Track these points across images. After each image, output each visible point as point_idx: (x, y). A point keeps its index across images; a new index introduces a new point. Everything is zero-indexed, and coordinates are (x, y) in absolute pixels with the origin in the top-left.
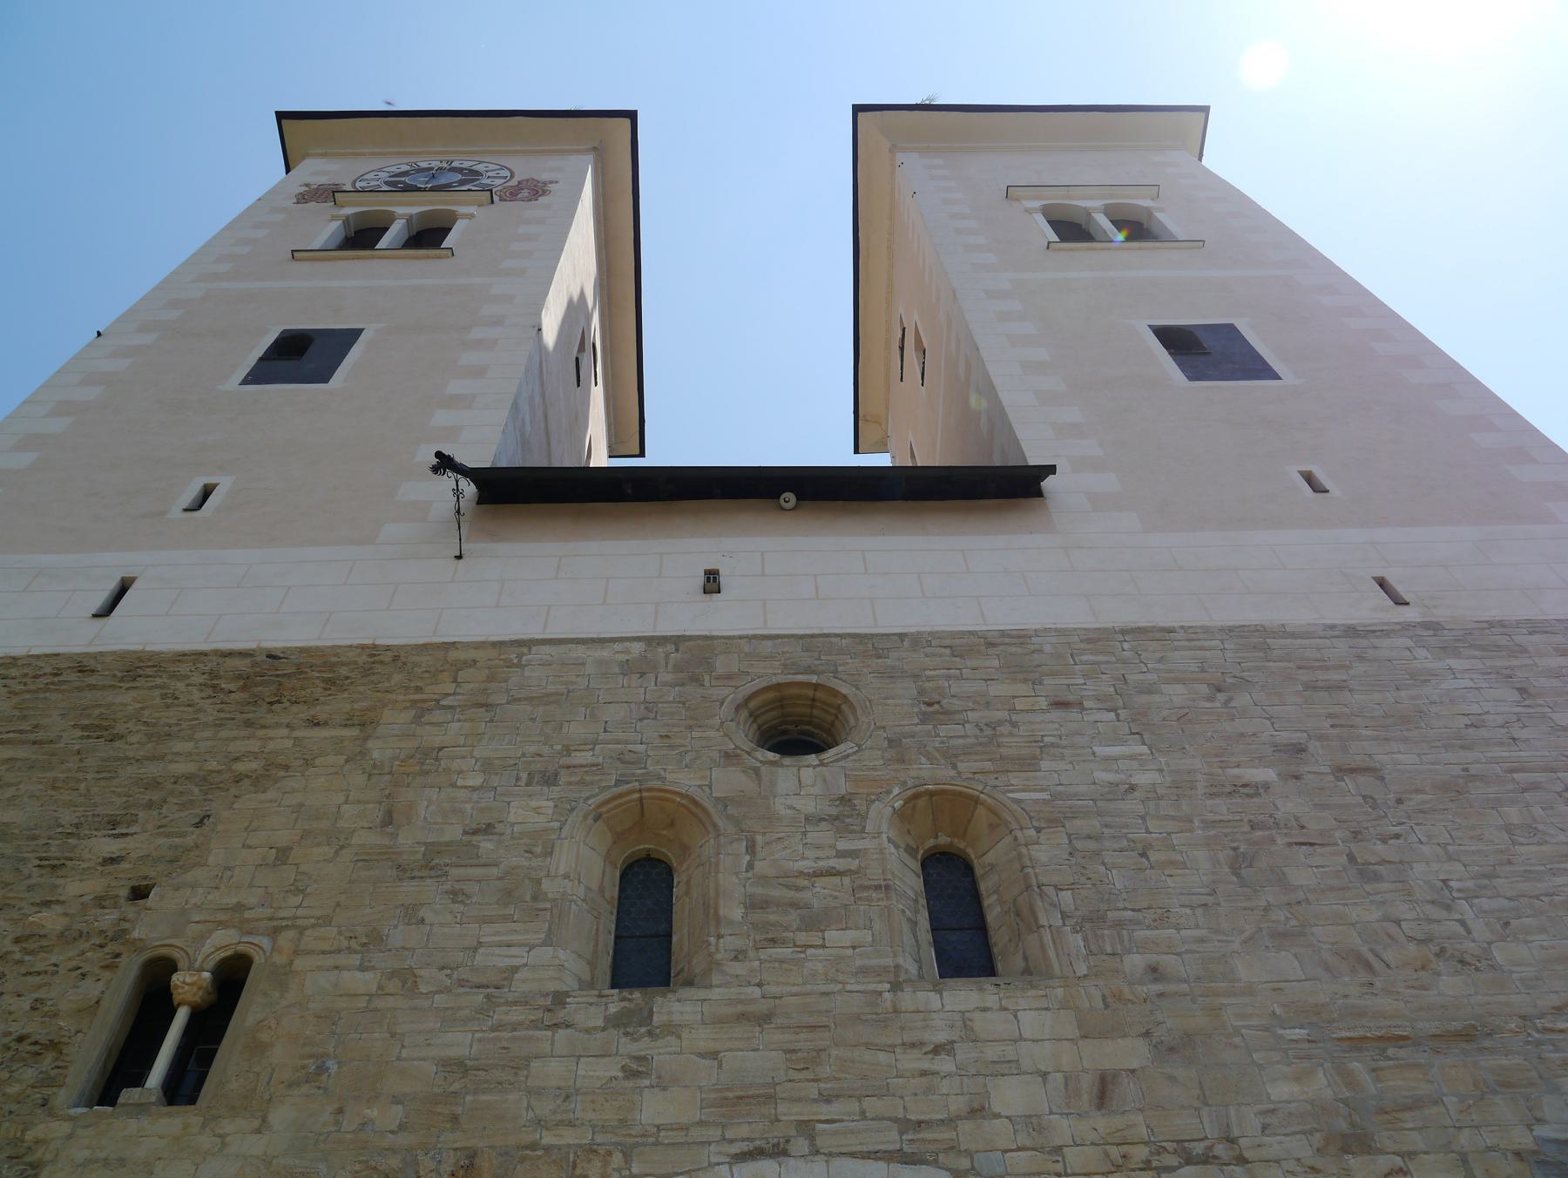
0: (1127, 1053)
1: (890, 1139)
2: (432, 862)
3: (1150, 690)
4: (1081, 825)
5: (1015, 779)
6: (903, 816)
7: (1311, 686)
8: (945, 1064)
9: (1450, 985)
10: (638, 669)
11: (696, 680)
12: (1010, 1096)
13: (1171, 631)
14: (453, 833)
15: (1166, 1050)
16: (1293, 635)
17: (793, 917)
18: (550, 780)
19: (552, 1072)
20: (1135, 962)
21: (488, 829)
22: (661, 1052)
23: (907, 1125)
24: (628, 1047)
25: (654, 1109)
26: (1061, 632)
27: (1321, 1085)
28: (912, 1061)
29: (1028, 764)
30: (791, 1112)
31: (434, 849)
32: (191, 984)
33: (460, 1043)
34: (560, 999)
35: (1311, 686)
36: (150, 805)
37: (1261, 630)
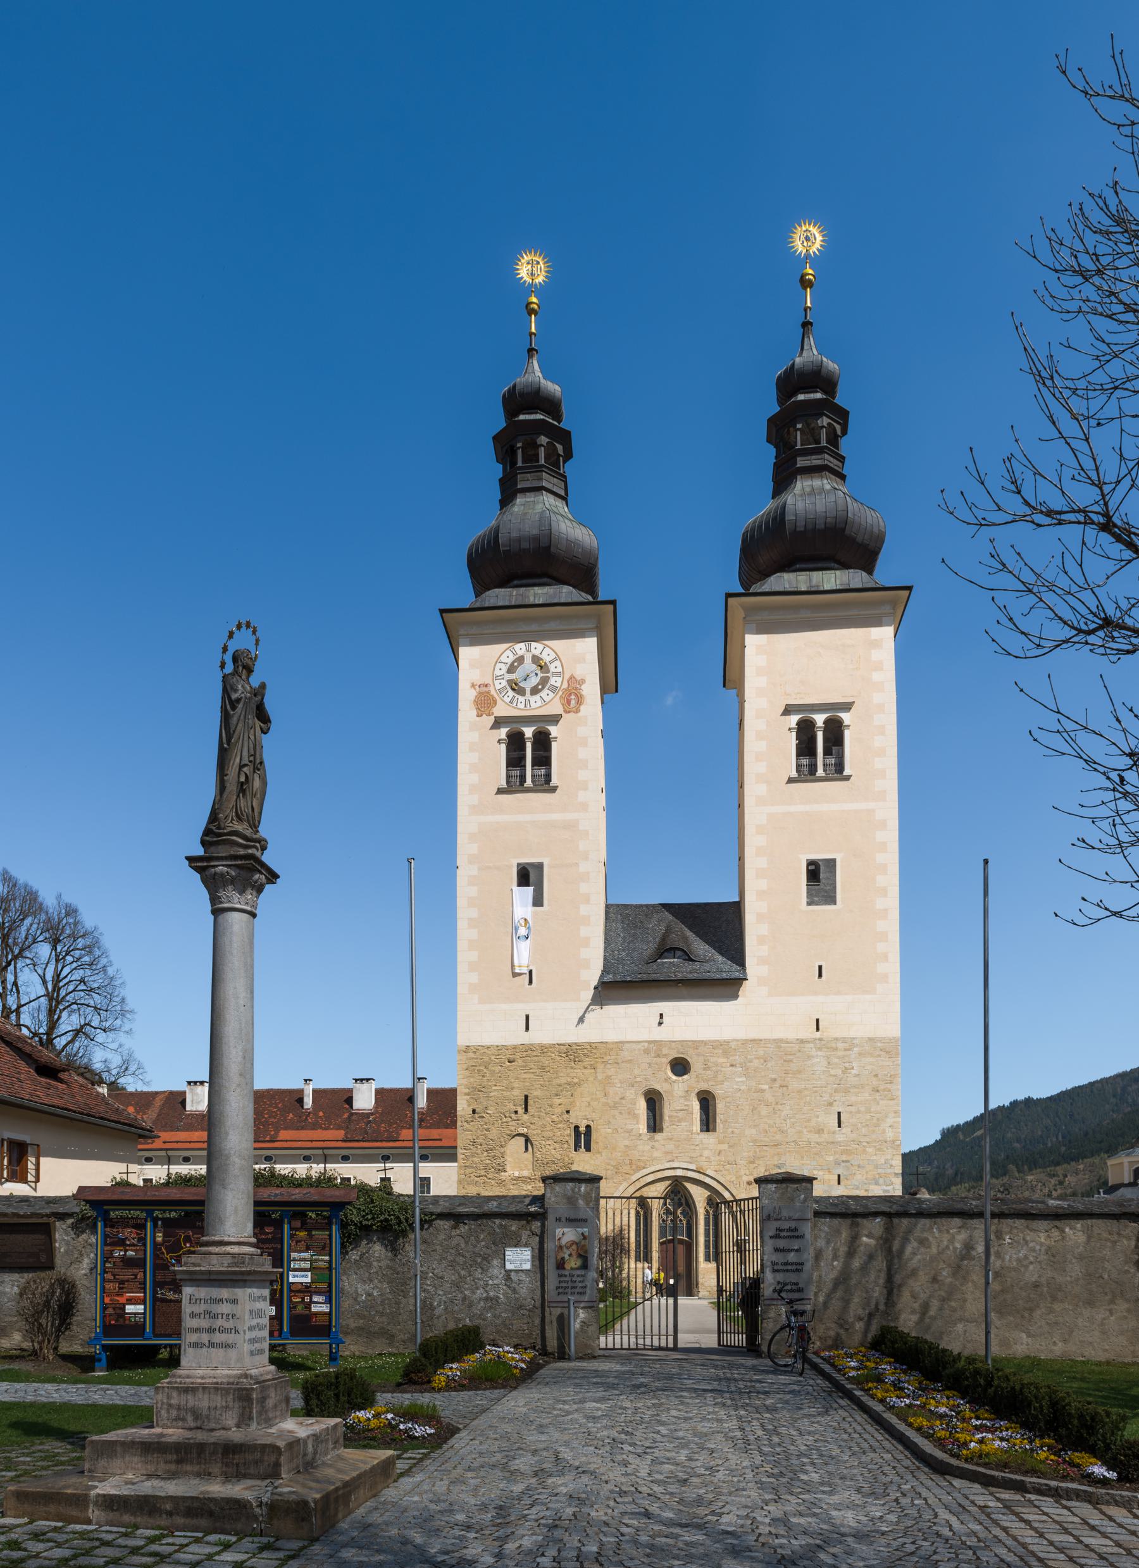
0: (725, 1147)
1: (689, 1160)
2: (615, 1106)
3: (751, 1061)
4: (728, 1100)
5: (718, 1087)
6: (698, 1094)
7: (785, 1061)
8: (697, 1148)
9: (779, 1137)
10: (647, 1051)
11: (658, 1056)
12: (706, 1153)
13: (761, 1040)
14: (617, 1099)
15: (730, 1147)
16: (788, 1043)
17: (676, 1119)
18: (633, 1086)
19: (641, 1148)
20: (730, 1130)
21: (622, 1098)
22: (656, 1144)
23: (691, 1157)
24: (651, 1144)
25: (656, 1154)
26: (738, 1041)
27: (751, 1154)
28: (693, 1147)
29: (722, 1083)
30: (675, 1155)
31: (615, 1103)
32: (582, 1129)
33: (627, 1143)
34: (640, 1135)
35: (785, 1061)
36: (562, 1091)
37: (782, 1041)
